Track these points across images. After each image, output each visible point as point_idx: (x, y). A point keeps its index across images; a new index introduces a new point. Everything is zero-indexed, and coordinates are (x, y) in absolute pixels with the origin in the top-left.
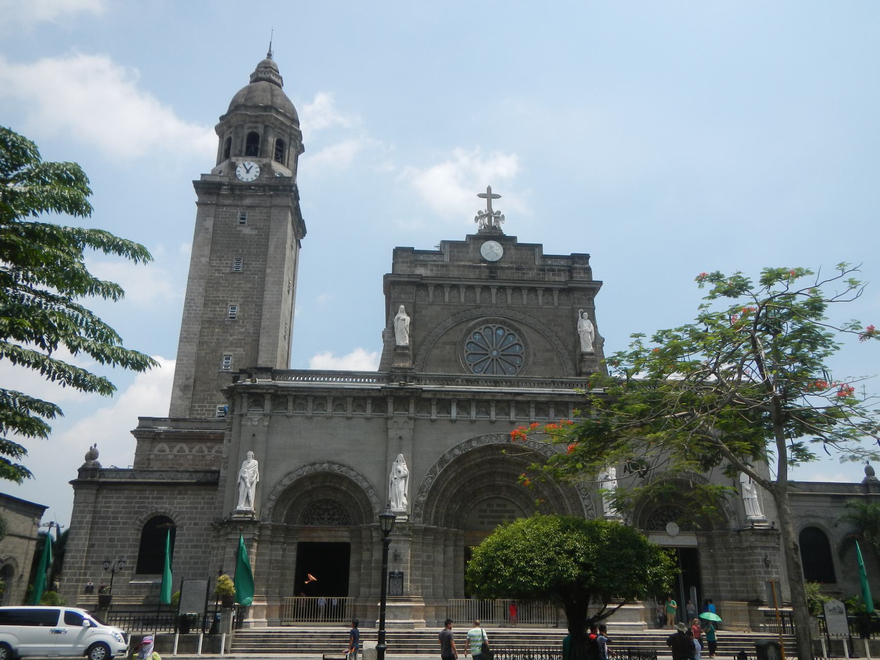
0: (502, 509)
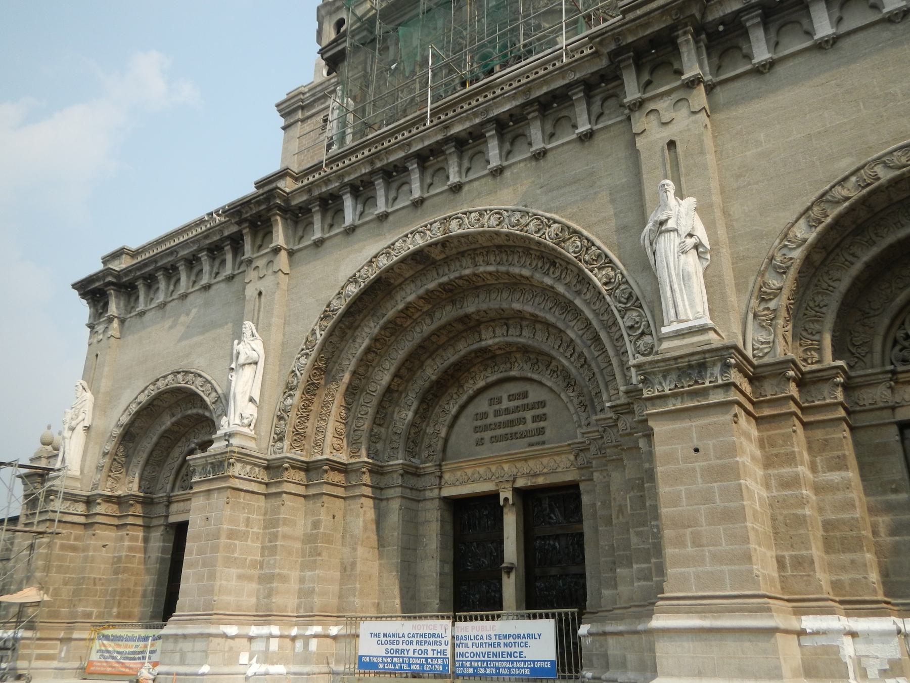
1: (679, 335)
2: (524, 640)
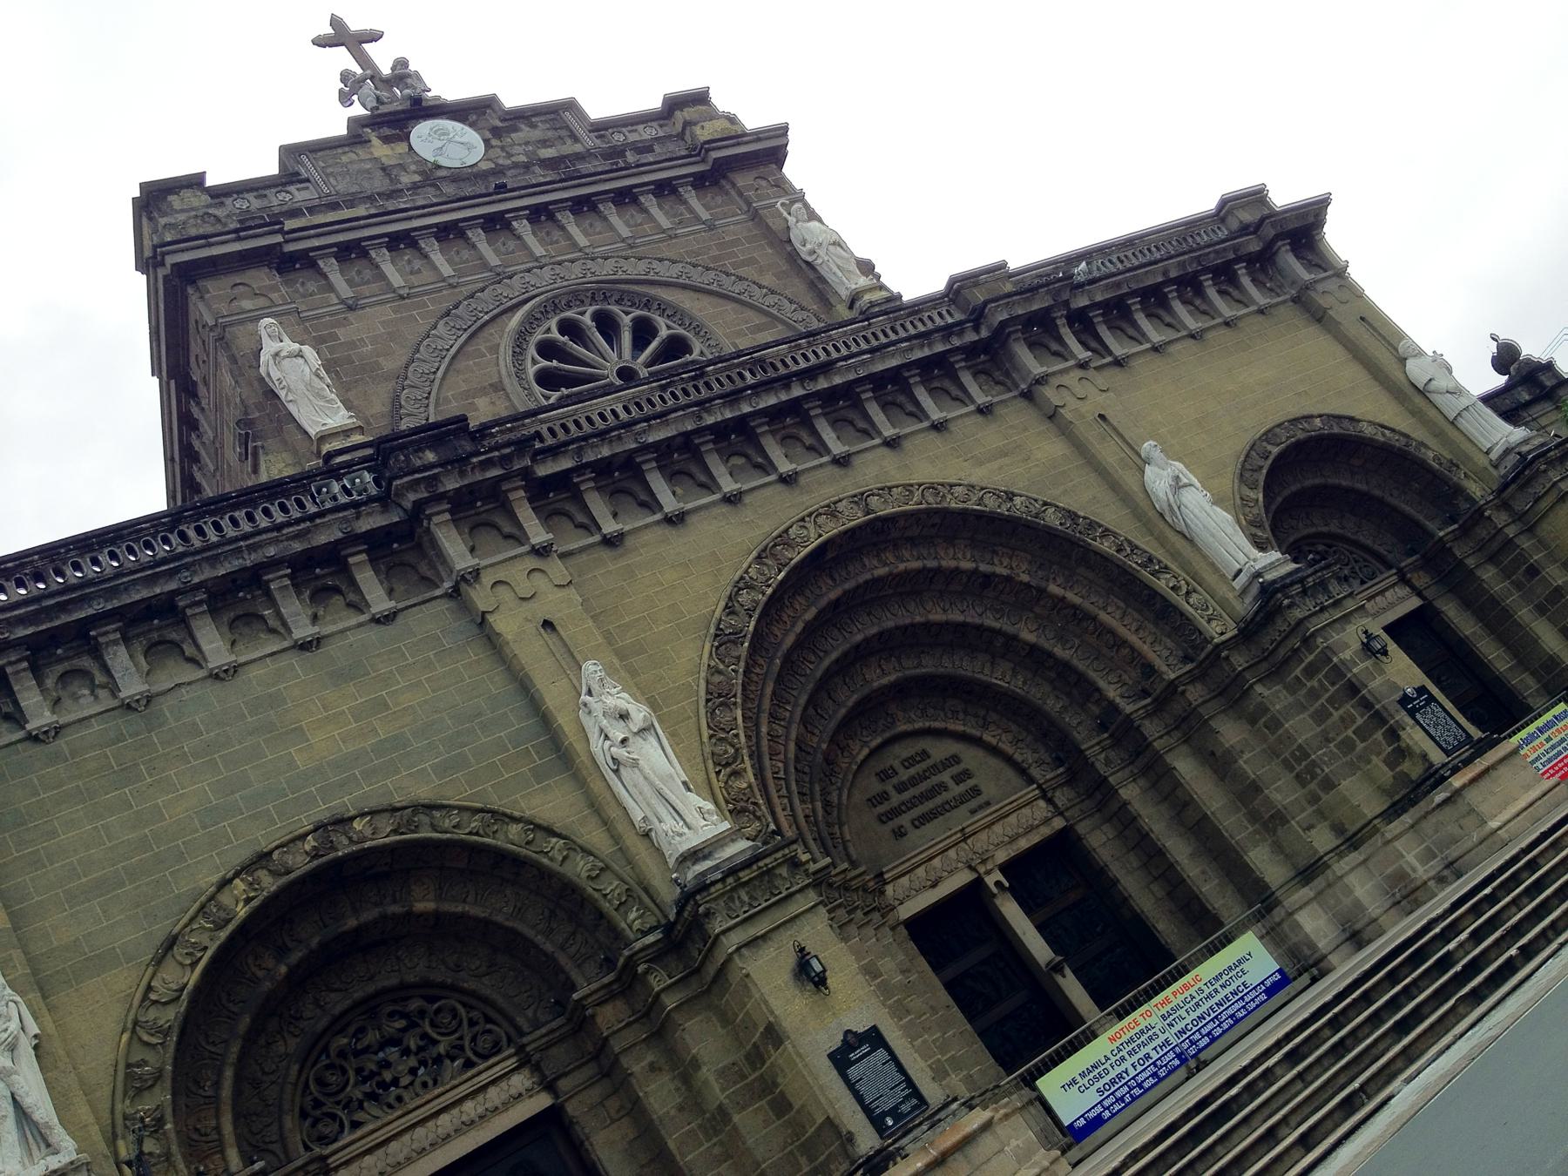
0: (924, 765)
1: (1272, 566)
2: (1238, 969)
